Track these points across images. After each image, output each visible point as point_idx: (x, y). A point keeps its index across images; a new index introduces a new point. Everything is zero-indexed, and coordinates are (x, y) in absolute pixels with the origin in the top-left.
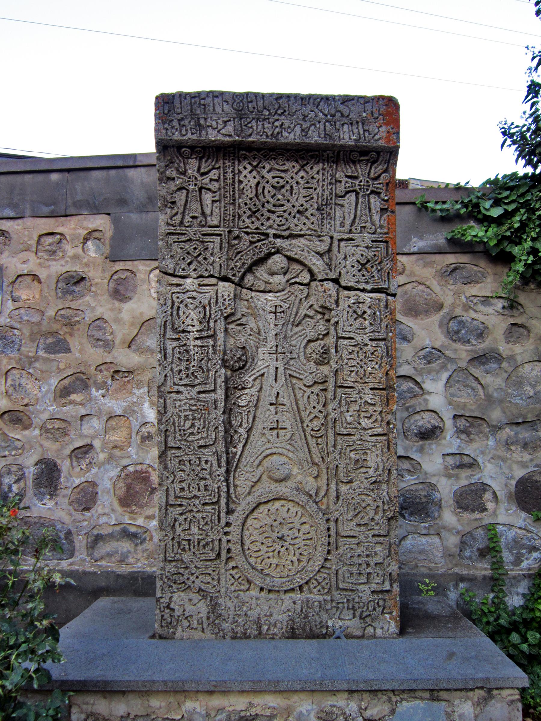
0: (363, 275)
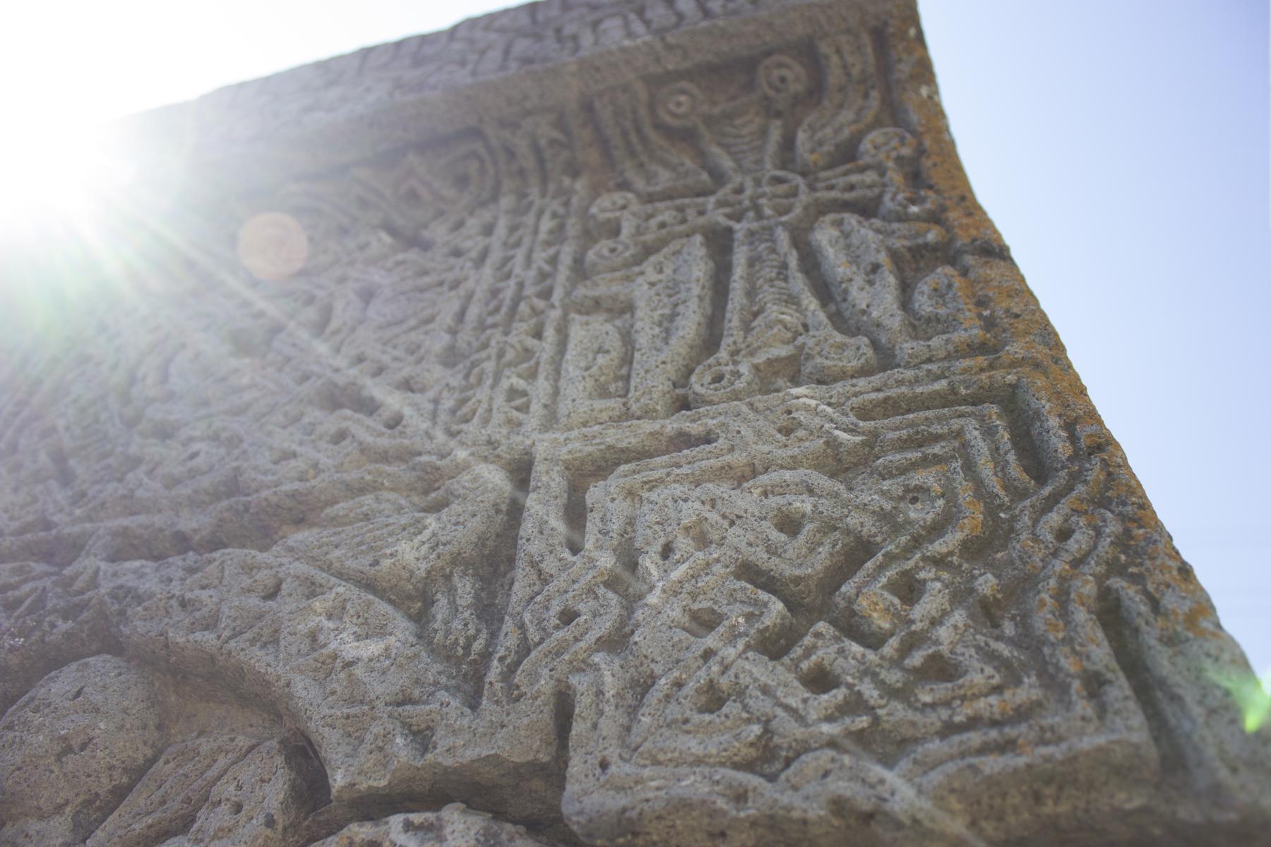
0: (820, 680)
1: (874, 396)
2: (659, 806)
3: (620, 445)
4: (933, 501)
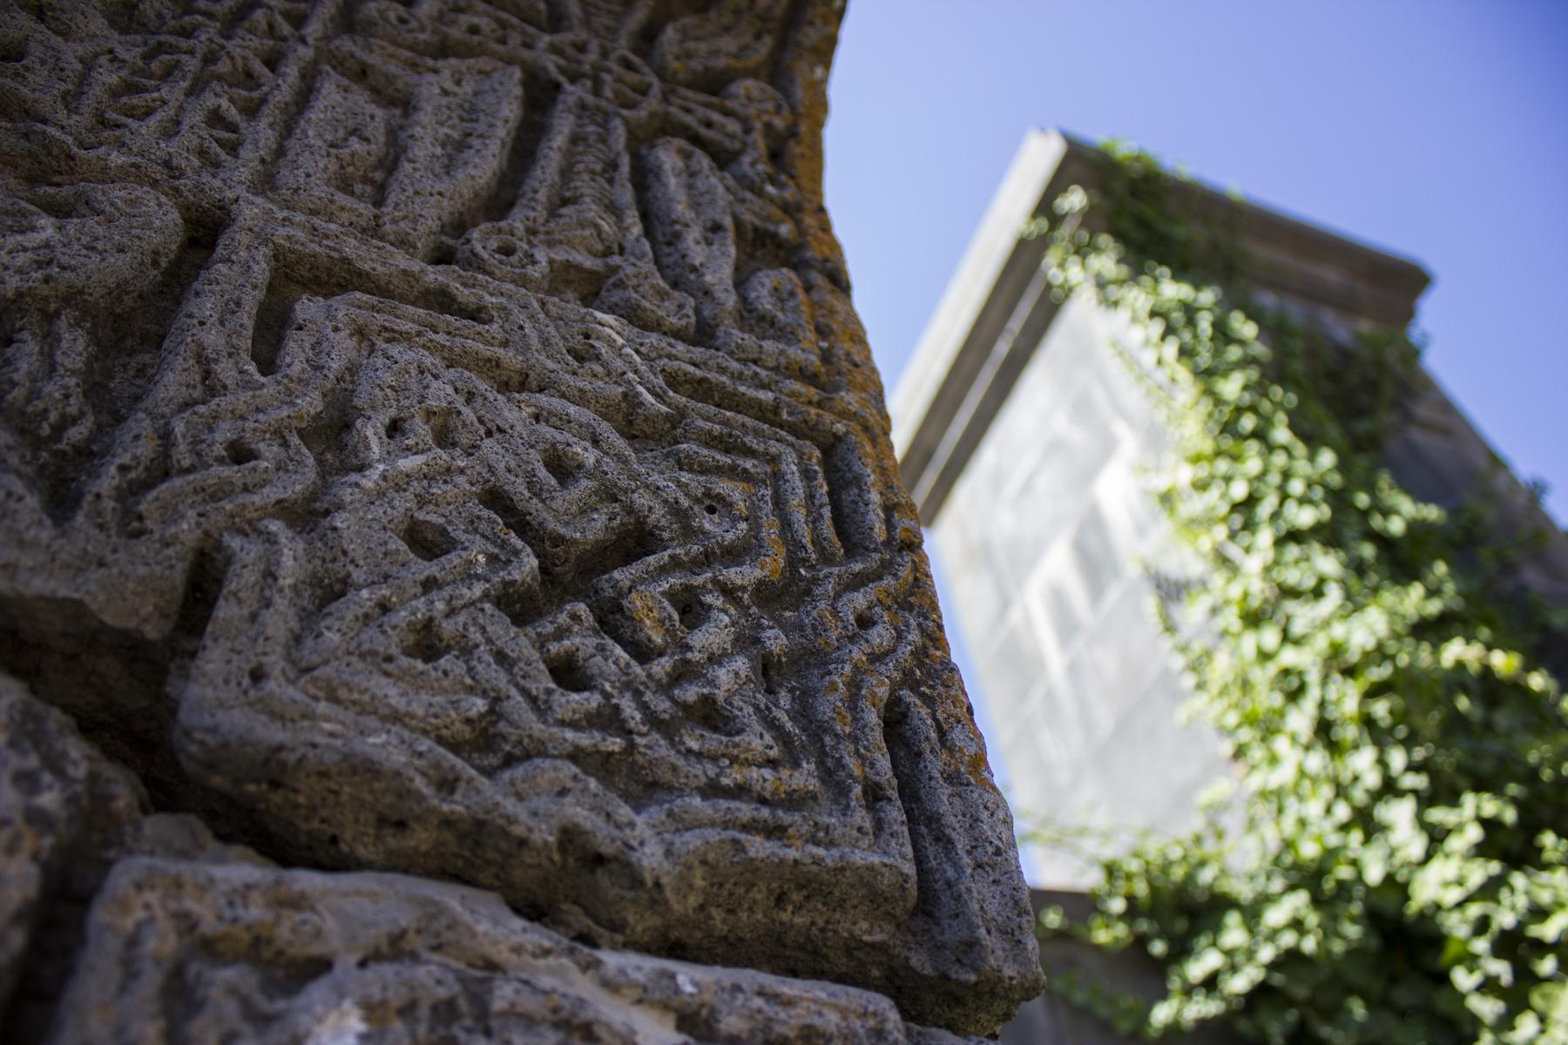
0: (569, 674)
1: (691, 369)
2: (330, 758)
3: (359, 264)
4: (735, 520)
